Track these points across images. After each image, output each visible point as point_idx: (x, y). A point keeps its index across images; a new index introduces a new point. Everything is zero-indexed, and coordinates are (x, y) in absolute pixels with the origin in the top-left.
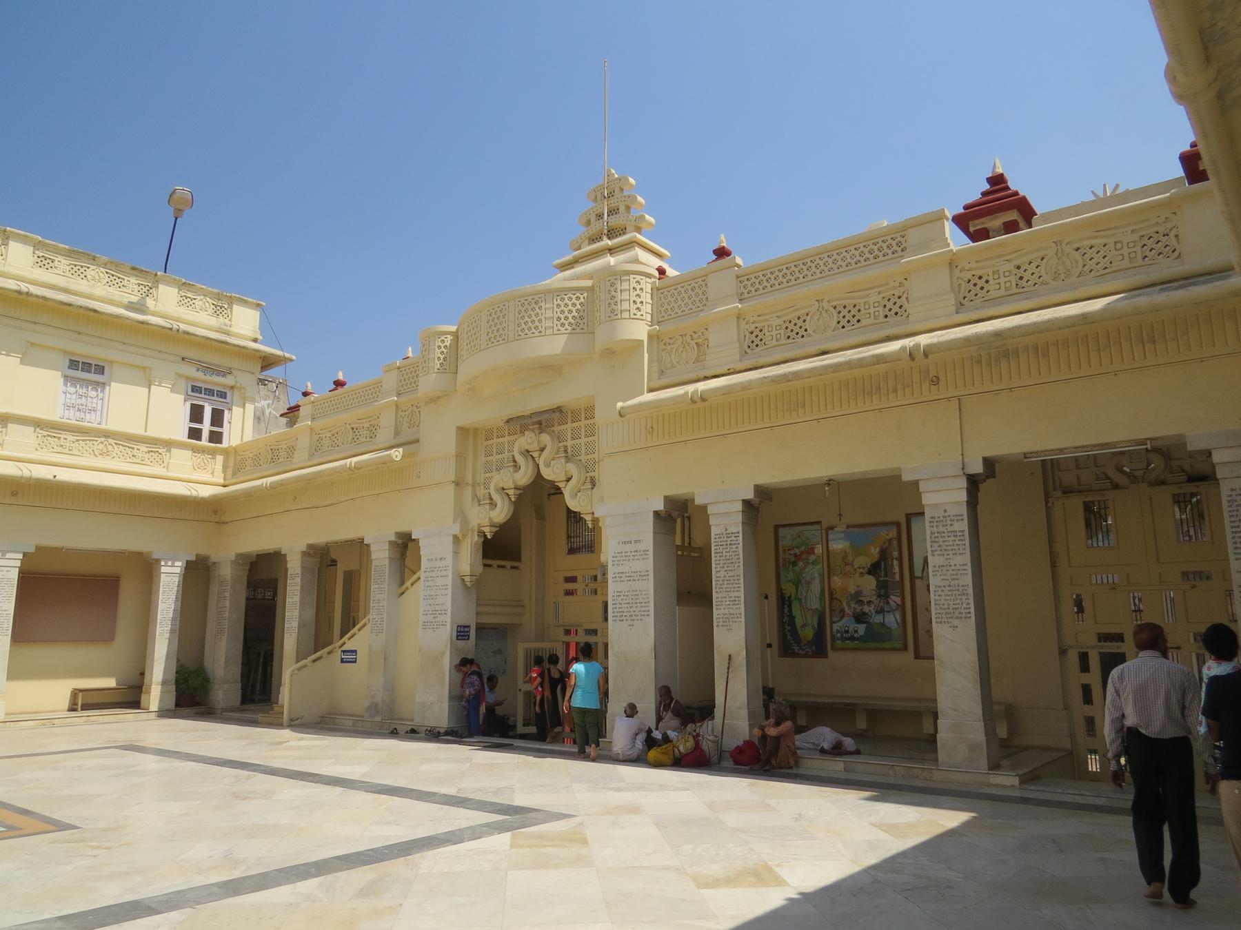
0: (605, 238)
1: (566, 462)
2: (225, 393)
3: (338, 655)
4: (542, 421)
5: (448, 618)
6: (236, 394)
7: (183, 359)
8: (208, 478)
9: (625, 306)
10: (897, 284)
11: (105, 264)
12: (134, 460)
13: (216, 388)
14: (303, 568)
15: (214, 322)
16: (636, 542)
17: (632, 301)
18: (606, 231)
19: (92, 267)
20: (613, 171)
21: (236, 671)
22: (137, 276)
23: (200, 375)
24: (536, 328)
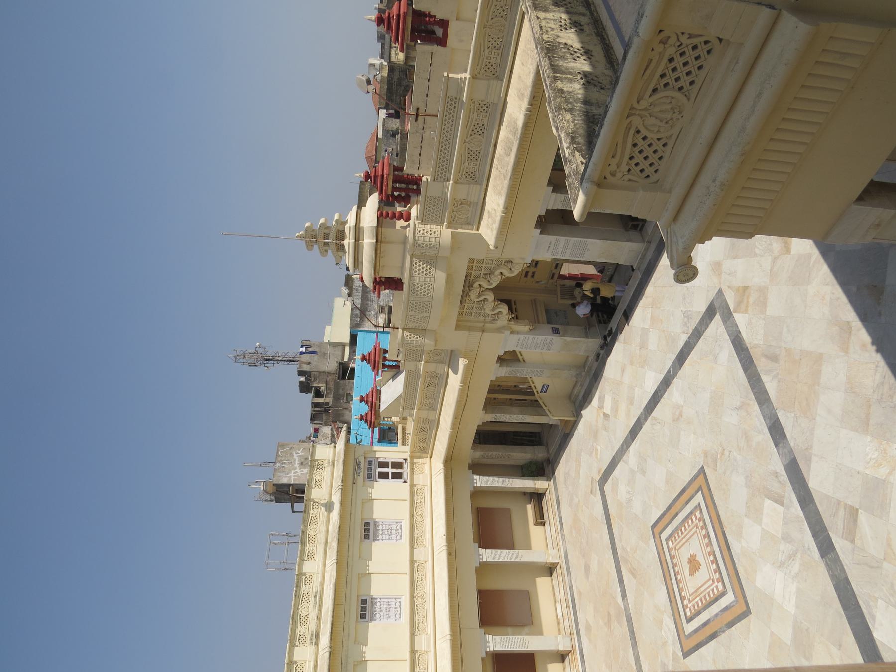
0: (343, 242)
1: (493, 274)
2: (369, 461)
3: (542, 394)
4: (469, 284)
5: (549, 338)
7: (354, 483)
8: (427, 467)
9: (433, 240)
10: (473, 104)
12: (423, 502)
13: (367, 467)
14: (493, 413)
15: (328, 470)
16: (550, 244)
18: (338, 242)
19: (308, 532)
20: (297, 235)
21: (528, 448)
22: (308, 511)
23: (362, 474)
24: (428, 286)
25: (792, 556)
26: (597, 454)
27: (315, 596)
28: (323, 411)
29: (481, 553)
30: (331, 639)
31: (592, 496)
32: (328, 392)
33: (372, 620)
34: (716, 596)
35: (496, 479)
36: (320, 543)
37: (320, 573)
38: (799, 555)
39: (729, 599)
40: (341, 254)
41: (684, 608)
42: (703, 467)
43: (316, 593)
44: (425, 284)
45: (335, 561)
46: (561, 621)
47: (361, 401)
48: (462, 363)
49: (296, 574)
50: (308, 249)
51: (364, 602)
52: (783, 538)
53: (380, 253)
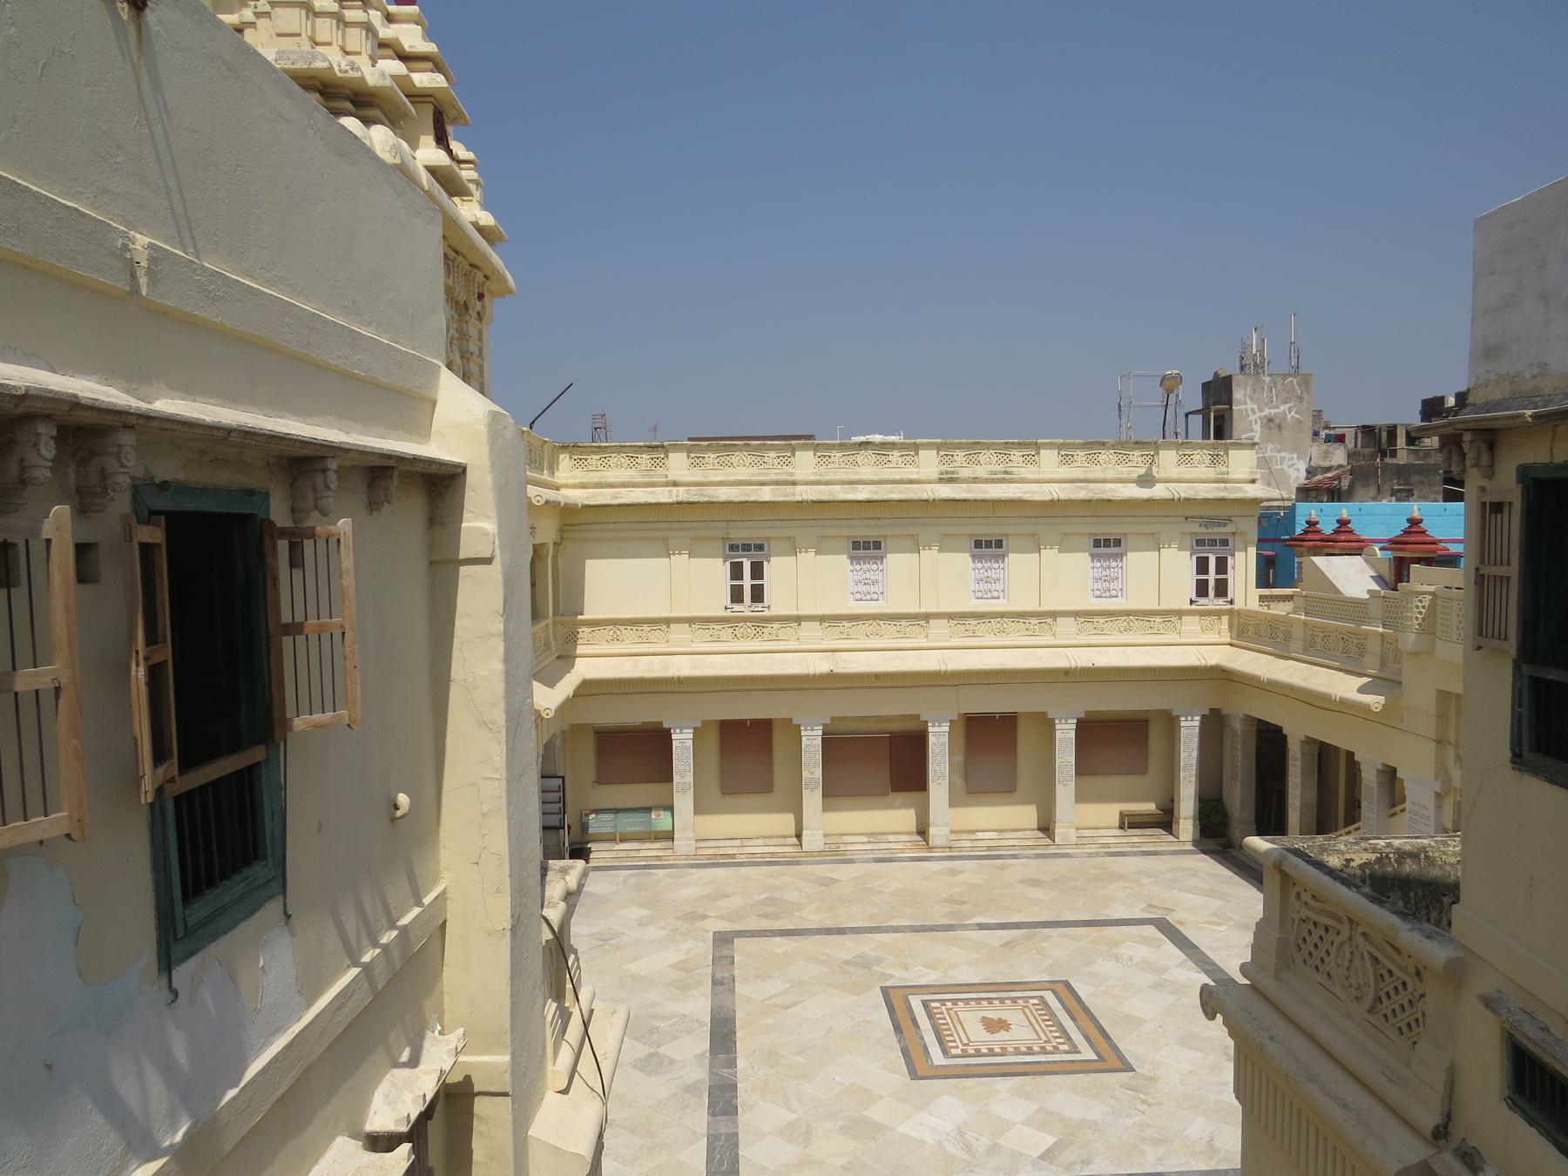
2: (1227, 540)
6: (1237, 537)
7: (1186, 518)
8: (1214, 638)
11: (1113, 446)
13: (1217, 537)
14: (1303, 754)
15: (1211, 473)
19: (1103, 452)
23: (1203, 530)
25: (968, 1148)
26: (1212, 923)
27: (1006, 473)
28: (1380, 447)
29: (1069, 721)
30: (945, 500)
31: (1145, 905)
32: (1421, 454)
33: (974, 557)
34: (945, 1043)
35: (1195, 754)
36: (1086, 472)
37: (1040, 476)
38: (966, 1157)
39: (938, 1058)
41: (943, 1002)
42: (1134, 1070)
43: (1011, 473)
45: (1056, 497)
46: (972, 837)
47: (1339, 521)
48: (1375, 701)
49: (1038, 441)
51: (999, 544)
52: (995, 1145)
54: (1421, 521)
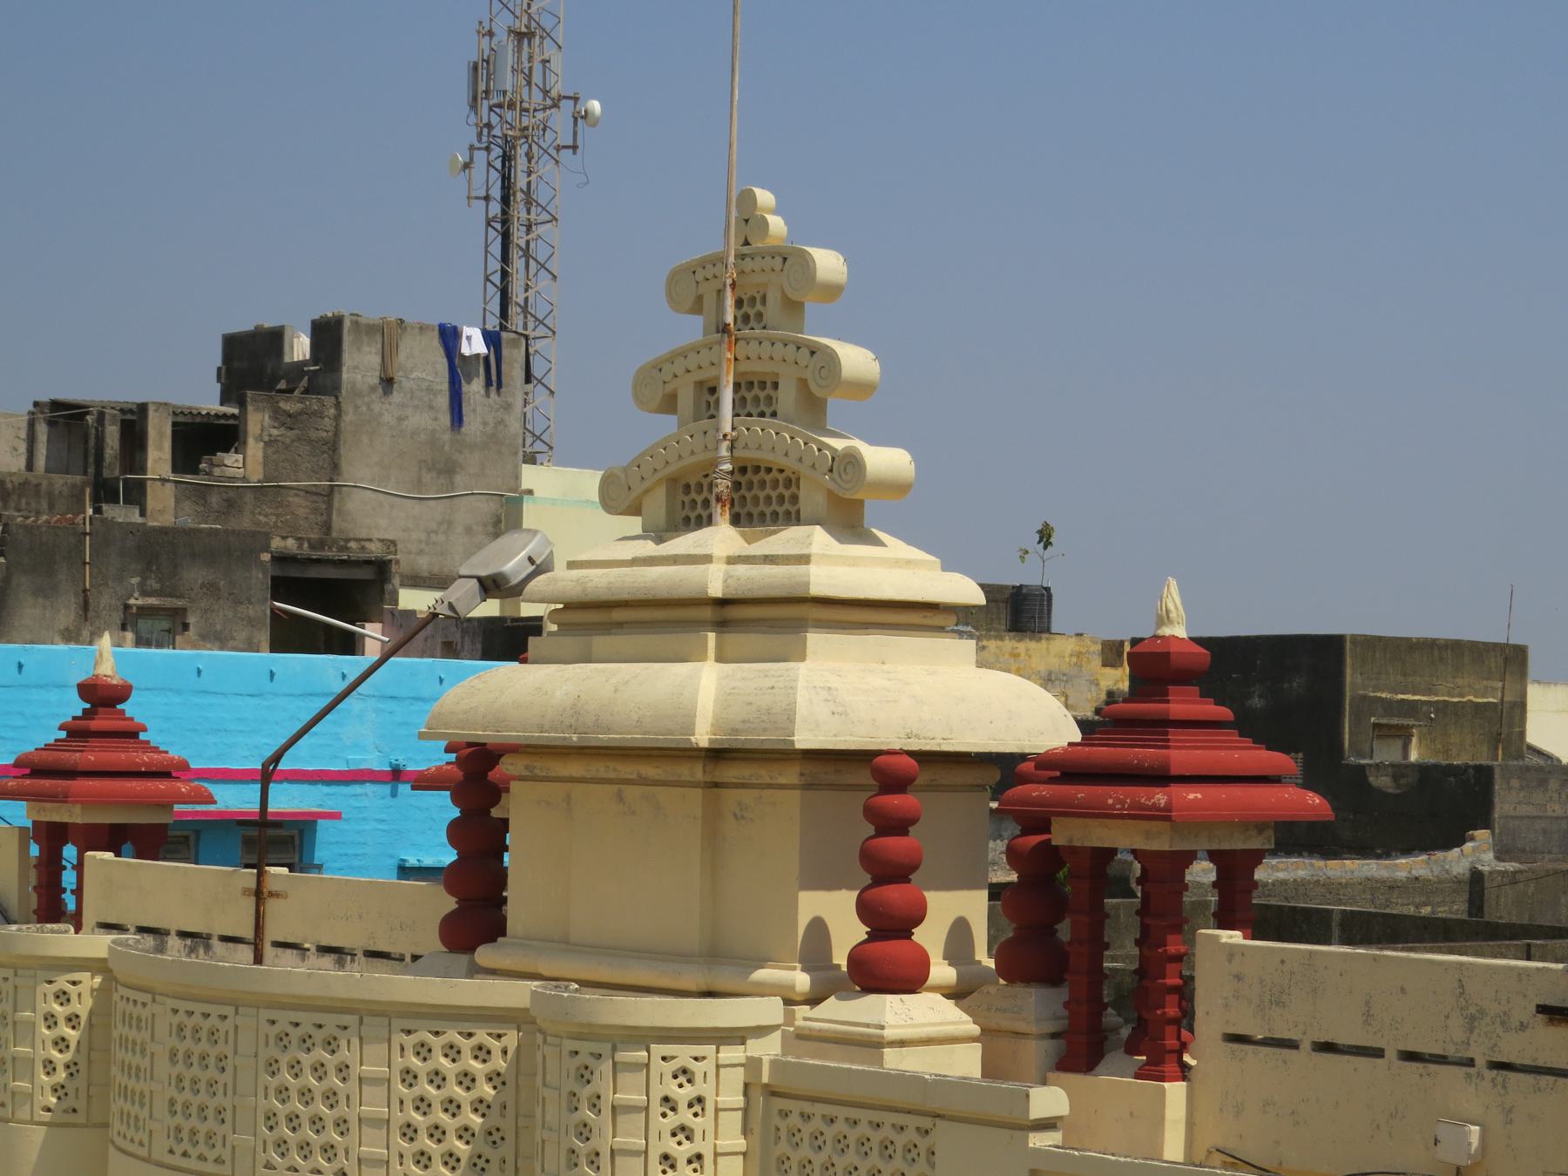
17: (654, 1158)
18: (723, 485)
20: (764, 197)
32: (215, 500)
40: (657, 504)
44: (341, 1124)
50: (674, 278)
53: (643, 781)
54: (122, 693)
